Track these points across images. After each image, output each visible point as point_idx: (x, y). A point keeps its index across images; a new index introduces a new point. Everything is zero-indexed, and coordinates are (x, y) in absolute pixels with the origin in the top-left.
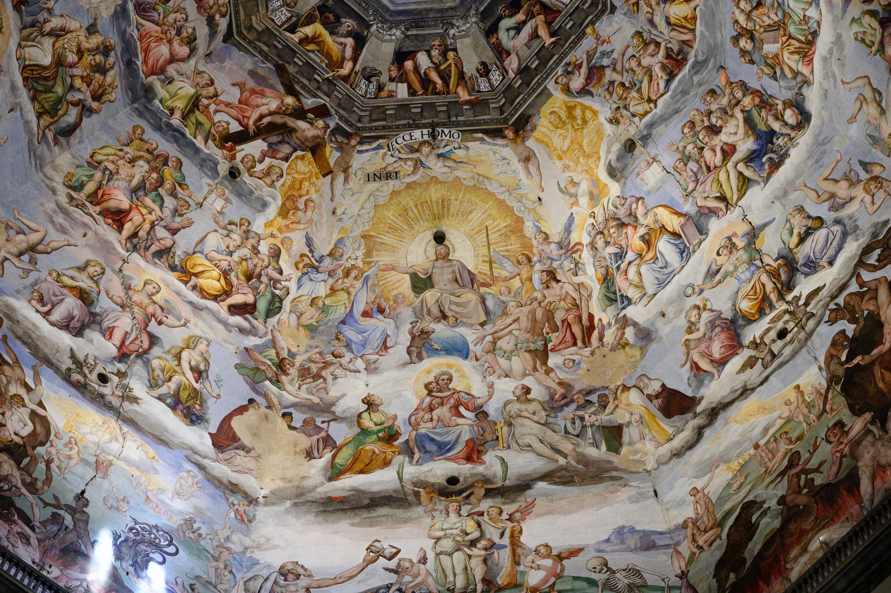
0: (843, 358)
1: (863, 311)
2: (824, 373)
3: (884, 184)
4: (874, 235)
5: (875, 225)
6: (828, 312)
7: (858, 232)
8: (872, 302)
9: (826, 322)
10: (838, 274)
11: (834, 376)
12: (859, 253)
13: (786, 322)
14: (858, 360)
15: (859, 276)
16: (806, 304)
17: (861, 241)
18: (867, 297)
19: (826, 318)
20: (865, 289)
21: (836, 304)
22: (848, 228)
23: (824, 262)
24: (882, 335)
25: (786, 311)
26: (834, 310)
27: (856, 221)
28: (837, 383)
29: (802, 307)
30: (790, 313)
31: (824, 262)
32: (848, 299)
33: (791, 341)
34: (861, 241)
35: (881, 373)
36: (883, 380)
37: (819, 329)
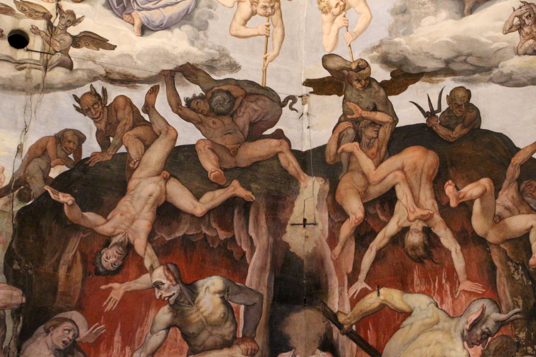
0: (54, 173)
1: (121, 143)
2: (19, 162)
3: (275, 17)
4: (212, 65)
5: (224, 54)
6: (87, 88)
7: (201, 34)
8: (140, 145)
9: (75, 97)
10: (140, 56)
11: (25, 183)
12: (181, 62)
13: (36, 31)
14: (65, 198)
15: (154, 91)
16: (76, 41)
17: (194, 50)
18: (140, 131)
19: (80, 92)
20: (146, 117)
21: (104, 91)
22: (197, 12)
23: (139, 16)
24: (113, 206)
25: (47, 17)
26: (97, 95)
27: (211, 17)
28: (22, 198)
29: (68, 39)
30: (50, 25)
31: (139, 16)
32: (121, 100)
33: (20, 65)
34: (194, 50)
35: (75, 256)
36: (69, 269)
37: (61, 94)
